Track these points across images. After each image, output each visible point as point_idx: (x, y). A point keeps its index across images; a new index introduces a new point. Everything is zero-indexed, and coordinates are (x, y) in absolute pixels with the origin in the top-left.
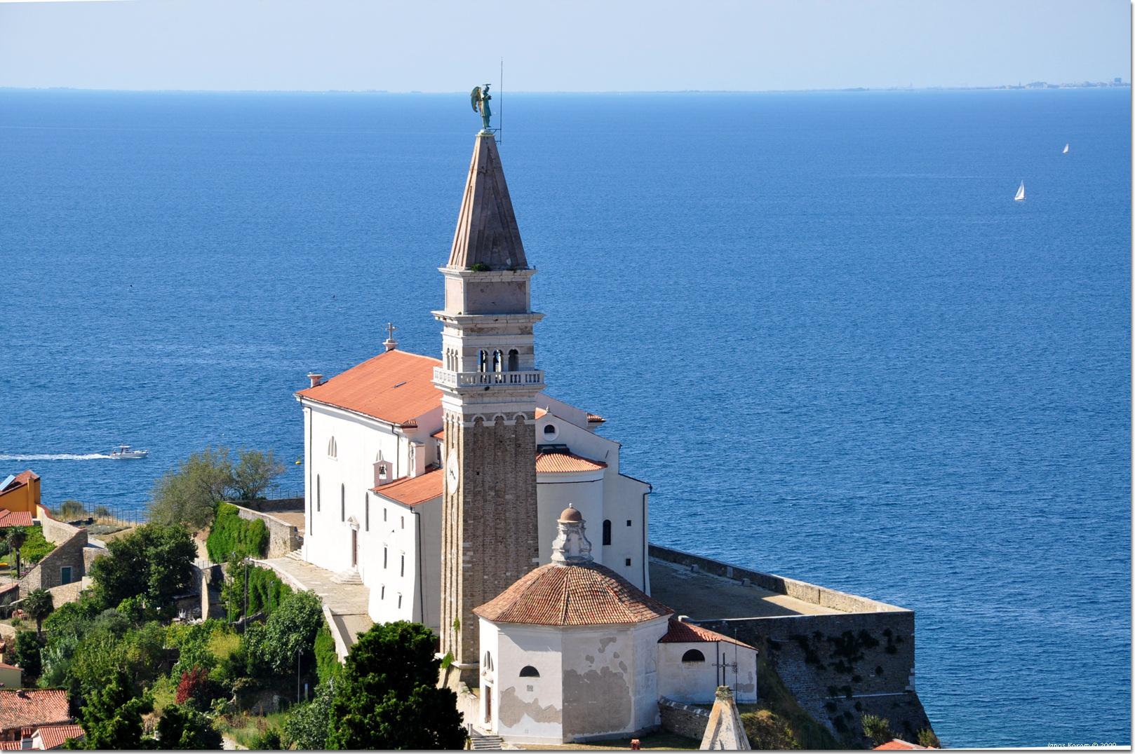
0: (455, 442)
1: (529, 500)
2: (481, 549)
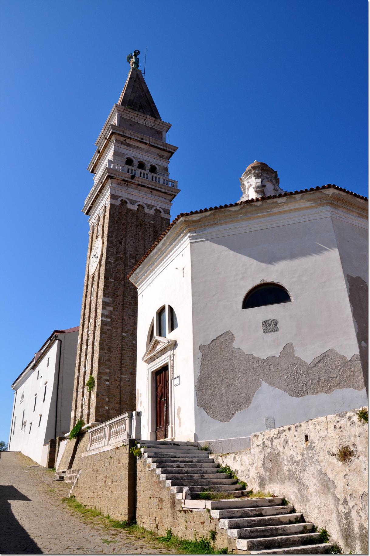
0: (100, 233)
2: (121, 307)
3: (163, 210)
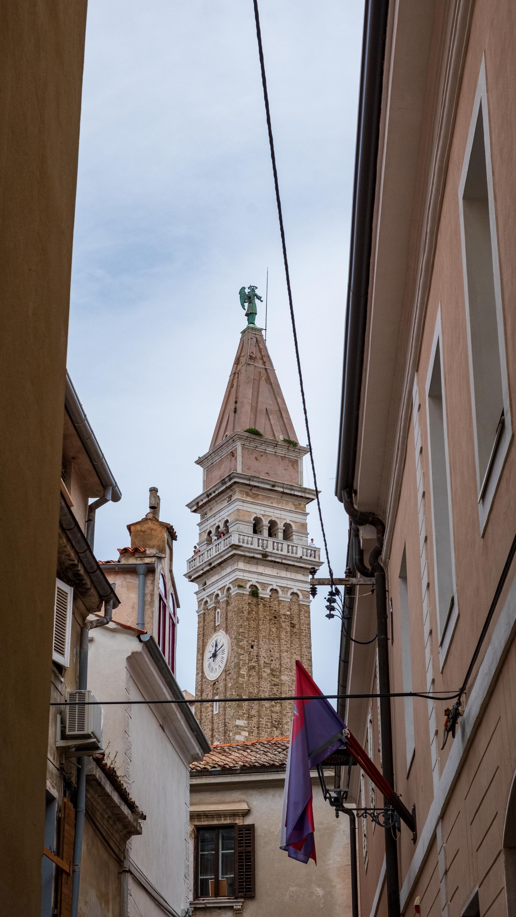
2: (256, 731)
3: (301, 592)
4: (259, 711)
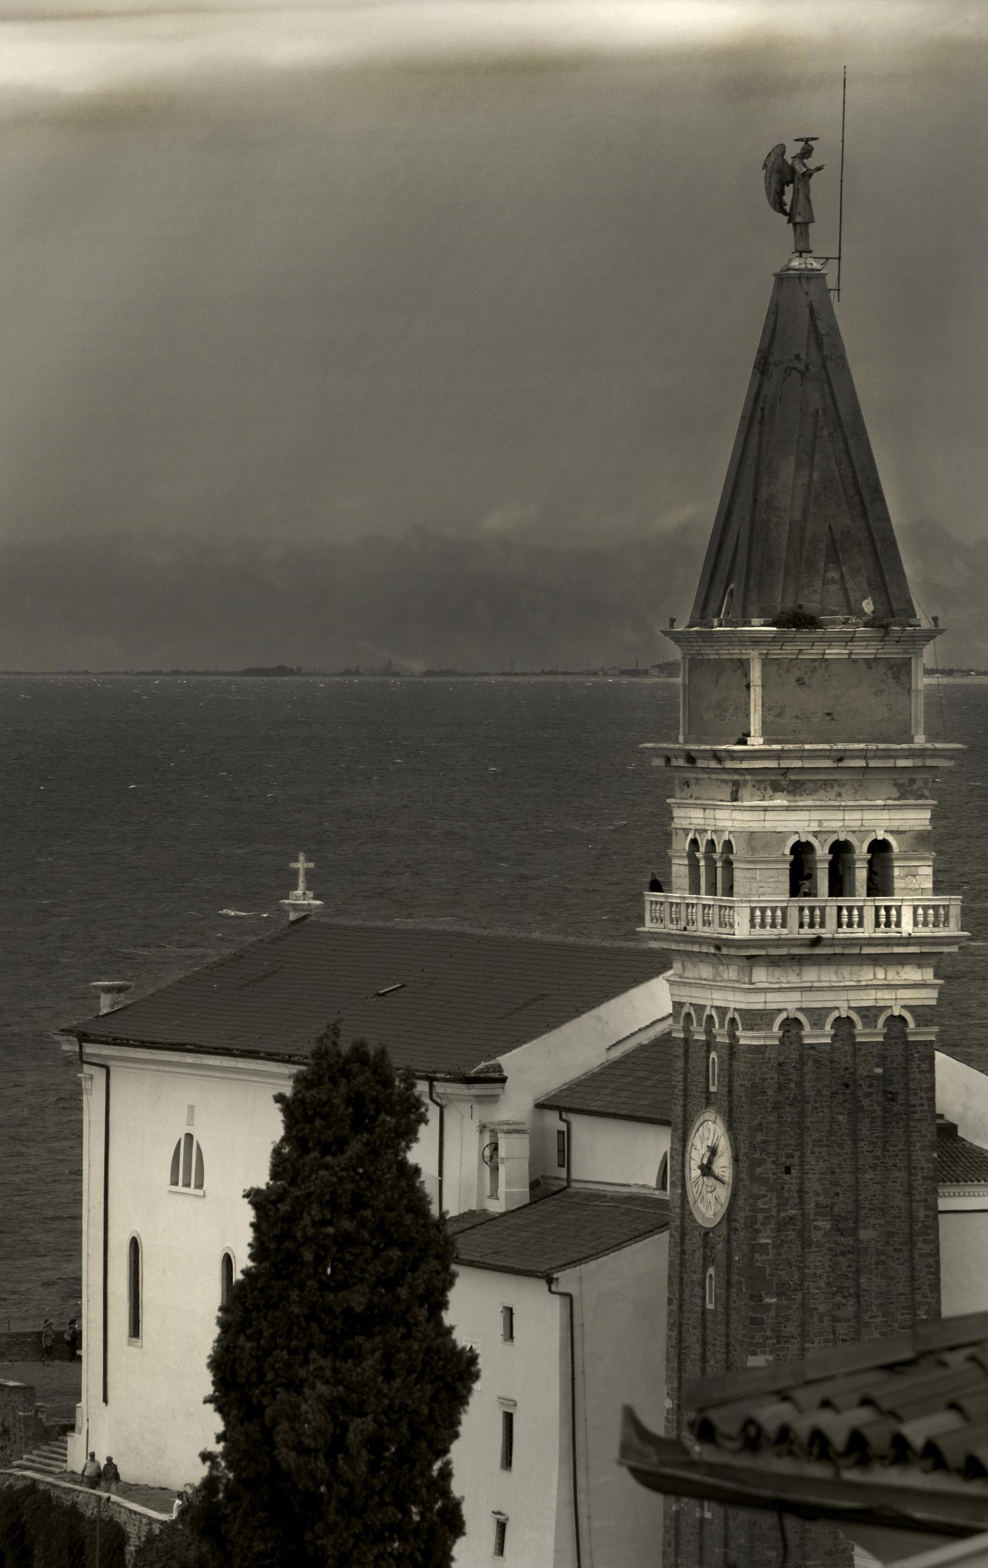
1: (919, 1245)
4: (802, 1325)
